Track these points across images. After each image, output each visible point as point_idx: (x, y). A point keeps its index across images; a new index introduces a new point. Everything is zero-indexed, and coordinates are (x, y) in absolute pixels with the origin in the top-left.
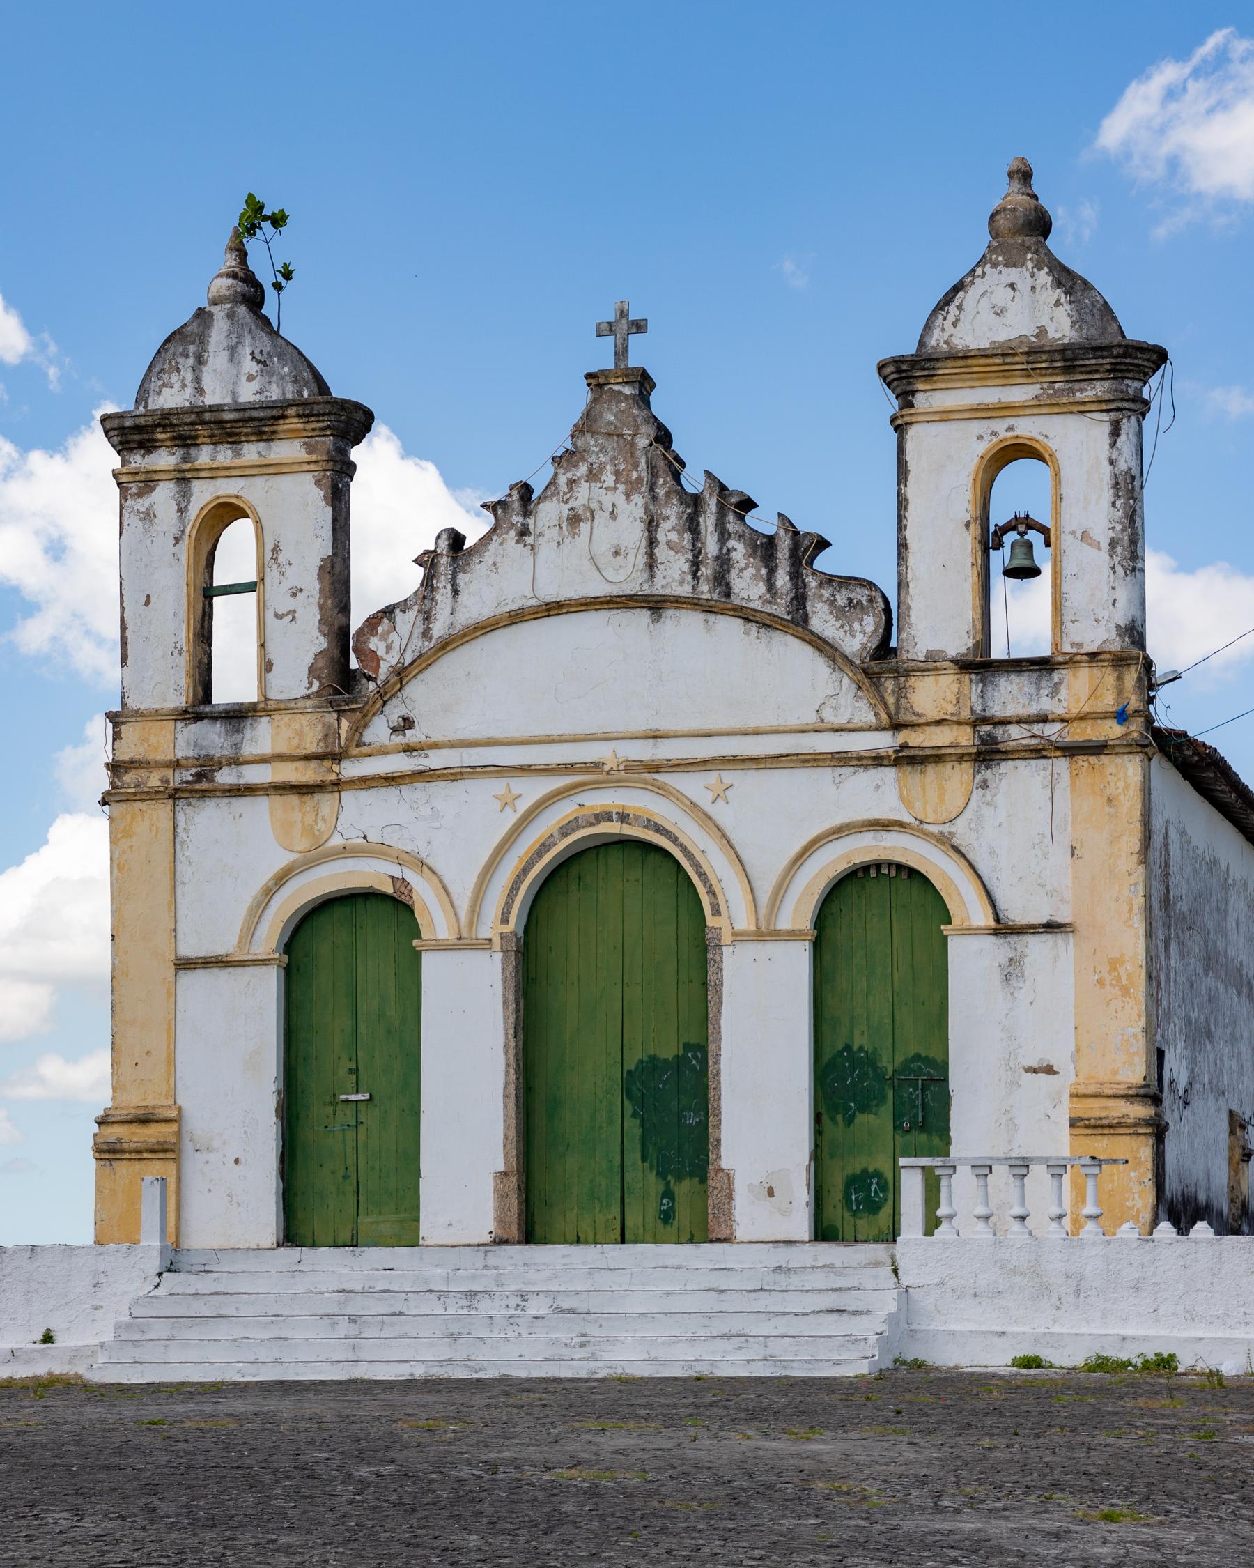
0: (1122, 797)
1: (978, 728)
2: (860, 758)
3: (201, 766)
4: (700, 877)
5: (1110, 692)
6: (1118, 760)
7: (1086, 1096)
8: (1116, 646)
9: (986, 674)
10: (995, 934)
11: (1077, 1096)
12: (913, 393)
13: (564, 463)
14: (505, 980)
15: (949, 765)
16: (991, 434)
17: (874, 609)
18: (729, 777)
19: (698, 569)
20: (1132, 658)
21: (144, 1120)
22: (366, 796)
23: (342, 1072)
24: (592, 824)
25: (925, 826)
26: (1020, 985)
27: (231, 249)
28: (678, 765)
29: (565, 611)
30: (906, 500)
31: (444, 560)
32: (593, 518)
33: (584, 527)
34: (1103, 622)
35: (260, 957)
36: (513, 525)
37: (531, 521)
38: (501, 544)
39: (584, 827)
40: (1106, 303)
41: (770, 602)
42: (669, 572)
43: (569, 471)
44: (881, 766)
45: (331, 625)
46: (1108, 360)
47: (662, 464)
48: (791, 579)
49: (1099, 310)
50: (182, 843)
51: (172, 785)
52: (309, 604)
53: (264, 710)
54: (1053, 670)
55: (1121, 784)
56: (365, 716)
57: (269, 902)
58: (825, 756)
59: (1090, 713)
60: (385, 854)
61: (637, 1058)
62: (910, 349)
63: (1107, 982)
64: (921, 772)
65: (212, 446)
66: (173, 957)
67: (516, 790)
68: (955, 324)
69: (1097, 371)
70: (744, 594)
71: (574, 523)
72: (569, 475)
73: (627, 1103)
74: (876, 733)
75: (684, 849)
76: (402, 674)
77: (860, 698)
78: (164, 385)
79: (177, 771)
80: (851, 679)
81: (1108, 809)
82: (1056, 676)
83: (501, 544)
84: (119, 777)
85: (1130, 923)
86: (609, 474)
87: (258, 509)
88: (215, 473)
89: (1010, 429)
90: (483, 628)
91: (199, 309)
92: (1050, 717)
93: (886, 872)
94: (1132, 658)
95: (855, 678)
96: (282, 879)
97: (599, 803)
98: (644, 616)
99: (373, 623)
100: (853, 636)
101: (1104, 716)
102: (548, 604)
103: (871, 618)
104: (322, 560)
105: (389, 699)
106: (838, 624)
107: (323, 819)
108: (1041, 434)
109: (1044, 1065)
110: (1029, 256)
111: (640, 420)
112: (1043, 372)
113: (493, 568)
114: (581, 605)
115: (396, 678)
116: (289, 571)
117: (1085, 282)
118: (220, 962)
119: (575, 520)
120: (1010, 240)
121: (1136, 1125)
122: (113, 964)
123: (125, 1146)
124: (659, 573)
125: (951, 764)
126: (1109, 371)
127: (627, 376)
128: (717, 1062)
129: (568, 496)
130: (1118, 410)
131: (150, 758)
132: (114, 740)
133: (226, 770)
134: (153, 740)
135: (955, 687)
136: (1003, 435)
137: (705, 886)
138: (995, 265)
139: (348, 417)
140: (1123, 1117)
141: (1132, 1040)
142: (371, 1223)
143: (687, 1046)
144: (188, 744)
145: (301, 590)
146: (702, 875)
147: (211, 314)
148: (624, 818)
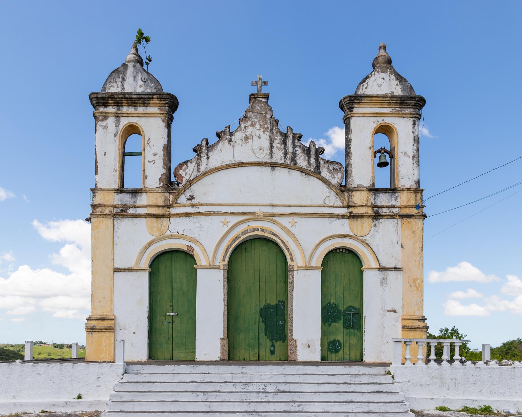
0: (417, 231)
1: (373, 209)
2: (338, 215)
3: (123, 207)
4: (287, 249)
5: (413, 200)
6: (416, 220)
7: (407, 319)
8: (415, 186)
9: (376, 193)
10: (379, 270)
11: (404, 319)
12: (353, 108)
13: (243, 121)
14: (224, 279)
15: (365, 219)
16: (377, 122)
17: (341, 171)
18: (296, 219)
19: (286, 156)
20: (420, 190)
21: (103, 319)
22: (178, 220)
23: (168, 306)
24: (252, 232)
25: (357, 237)
26: (386, 286)
27: (133, 47)
28: (281, 215)
29: (244, 165)
30: (351, 140)
31: (204, 148)
32: (253, 138)
33: (250, 141)
34: (411, 179)
35: (143, 269)
36: (227, 138)
37: (233, 138)
38: (223, 144)
39: (250, 232)
40: (411, 85)
41: (309, 167)
42: (277, 156)
43: (245, 123)
44: (344, 218)
45: (167, 166)
46: (414, 102)
47: (275, 123)
48: (315, 161)
49: (409, 88)
50: (116, 232)
51: (113, 213)
52: (160, 158)
53: (144, 191)
54: (396, 192)
55: (417, 227)
56: (179, 194)
57: (145, 251)
58: (327, 214)
59: (408, 206)
60: (185, 238)
61: (263, 305)
62: (353, 93)
63: (412, 286)
64: (356, 221)
65: (127, 107)
66: (113, 267)
67: (228, 221)
68: (366, 88)
69: (409, 105)
70: (301, 164)
71: (247, 139)
72: (245, 125)
73: (260, 318)
74: (342, 208)
75: (282, 241)
76: (191, 182)
77: (337, 198)
78: (111, 86)
79: (115, 209)
80: (334, 191)
81: (413, 235)
82: (397, 194)
83: (223, 144)
84: (95, 210)
85: (419, 268)
86: (258, 125)
88: (128, 115)
89: (383, 120)
90: (218, 169)
91: (124, 63)
92: (395, 206)
93: (342, 251)
94: (420, 190)
95: (336, 191)
96: (150, 244)
97: (255, 225)
98: (270, 168)
99: (180, 166)
100: (335, 179)
101: (412, 207)
102: (239, 163)
103: (340, 174)
104: (164, 145)
105: (186, 190)
106: (330, 175)
107: (164, 226)
108: (392, 123)
109: (393, 310)
110: (388, 70)
111: (268, 109)
112: (394, 104)
113: (220, 151)
114: (250, 164)
115: (189, 183)
116: (153, 148)
117: (405, 79)
118: (129, 270)
119: (247, 138)
120: (383, 65)
121: (422, 328)
122: (92, 269)
123: (97, 327)
124: (274, 156)
125: (365, 219)
126: (413, 105)
127: (264, 95)
128: (292, 306)
129: (245, 131)
130: (415, 117)
131: (105, 204)
132: (93, 198)
133: (131, 209)
134: (107, 198)
135: (366, 196)
136: (381, 122)
137: (288, 252)
138: (378, 72)
139: (173, 101)
140: (418, 326)
141: (419, 303)
142: (177, 353)
143: (279, 301)
144: (119, 200)
145: (157, 154)
146: (288, 249)
147: (127, 65)
148: (262, 230)
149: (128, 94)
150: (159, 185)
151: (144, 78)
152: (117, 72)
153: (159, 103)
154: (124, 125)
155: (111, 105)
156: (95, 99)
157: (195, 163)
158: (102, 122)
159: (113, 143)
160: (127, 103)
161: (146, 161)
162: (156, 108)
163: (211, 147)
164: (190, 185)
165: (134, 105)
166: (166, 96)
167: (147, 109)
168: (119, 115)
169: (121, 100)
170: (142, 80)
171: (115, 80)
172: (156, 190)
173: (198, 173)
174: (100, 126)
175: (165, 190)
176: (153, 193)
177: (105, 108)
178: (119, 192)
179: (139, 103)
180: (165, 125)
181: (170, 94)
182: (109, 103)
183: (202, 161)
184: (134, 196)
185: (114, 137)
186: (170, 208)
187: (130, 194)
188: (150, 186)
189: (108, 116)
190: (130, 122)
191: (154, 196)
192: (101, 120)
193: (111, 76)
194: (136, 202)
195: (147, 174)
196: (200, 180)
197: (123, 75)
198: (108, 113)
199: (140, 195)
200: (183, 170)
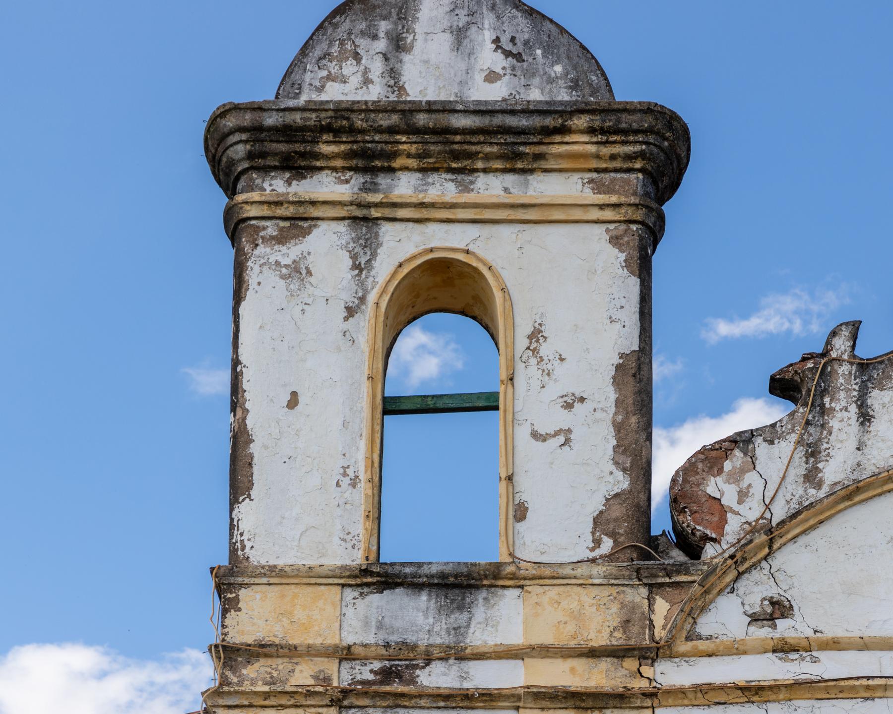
52: (596, 421)
65: (419, 175)
78: (330, 78)
87: (505, 274)
105: (748, 570)
116: (559, 370)
145: (582, 400)
149: (431, 108)
150: (592, 550)
151: (513, 40)
152: (363, 11)
153: (598, 157)
154: (402, 260)
155: (328, 168)
156: (244, 137)
157: (793, 440)
158: (276, 247)
159: (339, 349)
160: (419, 156)
161: (522, 434)
162: (576, 177)
163: (881, 362)
164: (767, 550)
165: (454, 165)
166: (637, 116)
167: (527, 184)
168: (375, 213)
169: (386, 143)
170: (498, 47)
171: (349, 46)
172: (579, 572)
173: (812, 491)
174: (265, 268)
175: (627, 573)
176: (562, 588)
177: (294, 182)
178: (368, 585)
179: (487, 157)
180: (625, 261)
181: (662, 107)
182: (317, 156)
183: (835, 431)
184: (452, 601)
185: (346, 319)
186: (654, 661)
187: (429, 595)
188: (542, 553)
189: (313, 219)
190: (432, 245)
191: (564, 604)
192: (272, 238)
193: (330, 31)
194: (462, 630)
195: (524, 498)
196: (821, 522)
197: (396, 24)
198: (313, 203)
199: (485, 599)
200: (724, 474)
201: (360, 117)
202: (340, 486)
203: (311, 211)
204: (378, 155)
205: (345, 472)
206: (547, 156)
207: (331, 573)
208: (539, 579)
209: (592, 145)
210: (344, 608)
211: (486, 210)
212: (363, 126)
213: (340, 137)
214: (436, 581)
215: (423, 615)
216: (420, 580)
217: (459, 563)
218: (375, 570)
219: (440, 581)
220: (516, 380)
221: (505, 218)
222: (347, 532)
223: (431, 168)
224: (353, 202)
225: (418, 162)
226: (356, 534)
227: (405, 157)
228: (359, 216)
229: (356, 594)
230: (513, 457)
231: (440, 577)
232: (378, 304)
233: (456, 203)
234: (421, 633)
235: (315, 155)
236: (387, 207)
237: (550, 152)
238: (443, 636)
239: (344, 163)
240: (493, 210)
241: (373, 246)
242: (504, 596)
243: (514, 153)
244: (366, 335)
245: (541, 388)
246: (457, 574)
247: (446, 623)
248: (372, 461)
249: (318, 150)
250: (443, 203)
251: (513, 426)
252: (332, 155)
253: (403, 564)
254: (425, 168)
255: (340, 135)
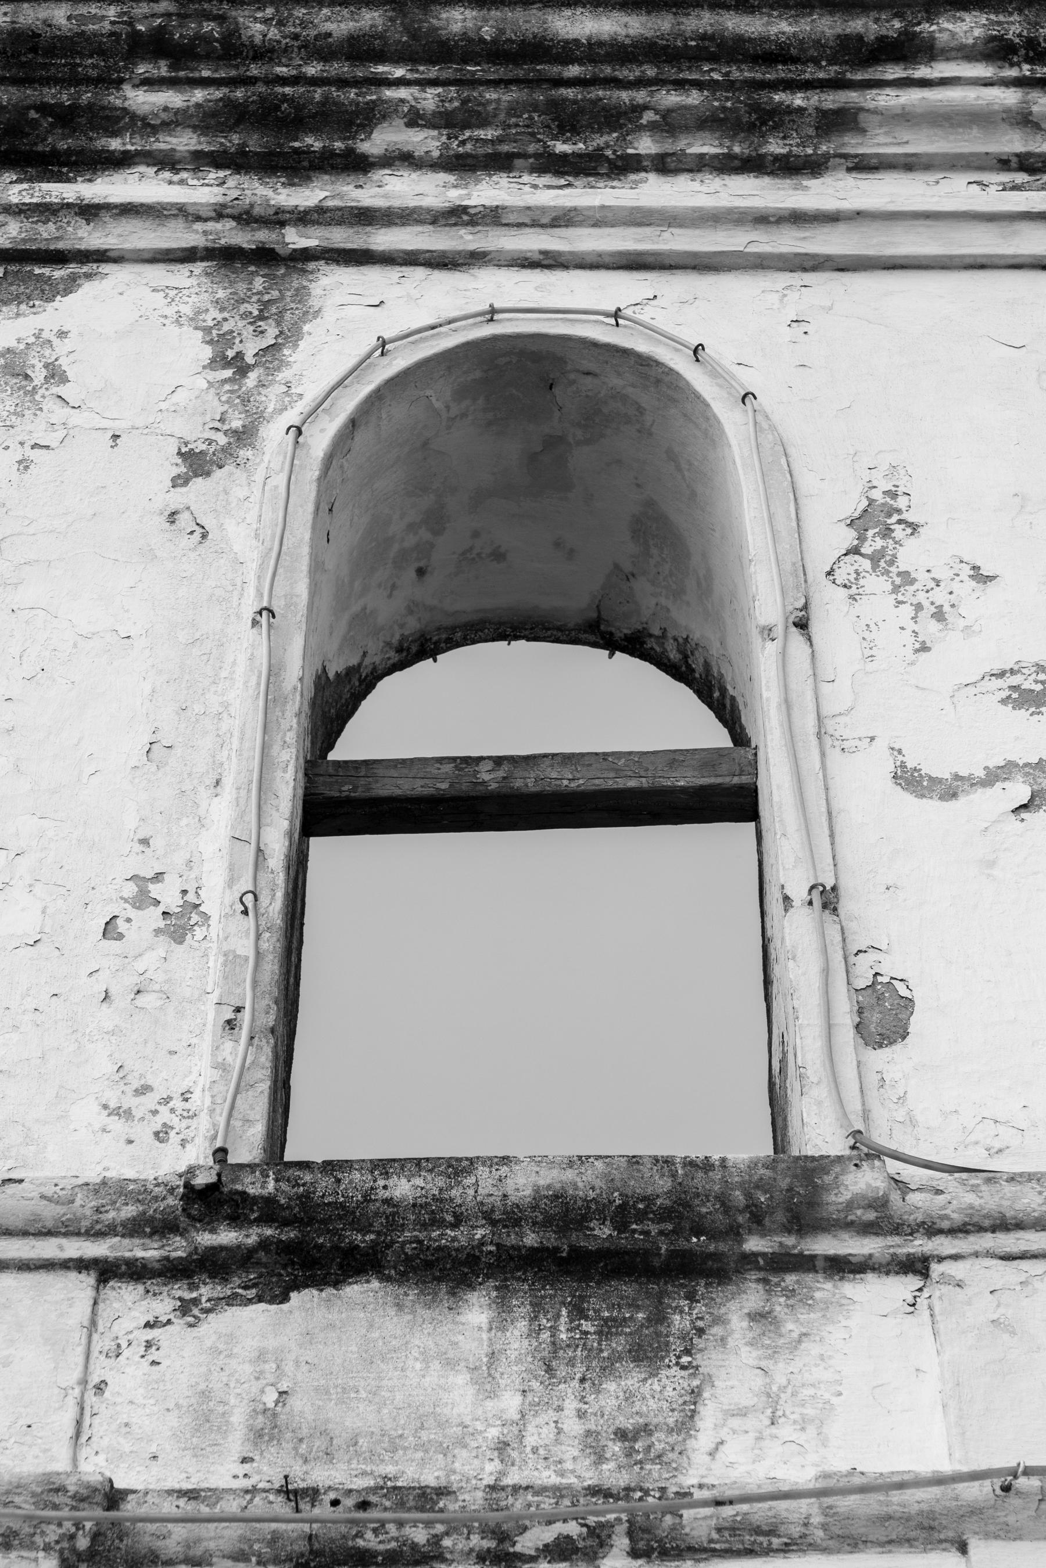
184: (607, 1329)
185: (179, 482)
187: (502, 1304)
194: (660, 1441)
199: (757, 1317)
201: (259, 15)
202: (120, 937)
203: (81, 233)
204: (314, 116)
205: (143, 893)
206: (862, 116)
207: (50, 1213)
208: (994, 1229)
209: (1003, 89)
210: (90, 1394)
211: (671, 229)
212: (270, 36)
213: (192, 70)
214: (531, 1239)
215: (474, 1382)
216: (460, 1236)
217: (634, 1161)
218: (251, 1191)
219: (551, 1239)
220: (815, 628)
221: (741, 249)
222: (136, 1084)
223: (487, 155)
224: (224, 206)
225: (444, 139)
226: (176, 1091)
227: (400, 122)
228: (245, 246)
229: (163, 1306)
230: (832, 836)
231: (547, 1223)
232: (300, 432)
233: (575, 209)
234: (464, 1453)
235: (107, 118)
236: (340, 223)
237: (871, 105)
238: (569, 1465)
239: (200, 143)
240: (697, 232)
241: (288, 316)
242: (844, 1304)
243: (755, 107)
244: (252, 517)
245: (917, 651)
246: (623, 1207)
247: (581, 1415)
248: (260, 852)
249: (118, 103)
250: (529, 208)
251: (823, 754)
252: (164, 116)
253: (383, 1167)
254: (467, 155)
255: (194, 64)
